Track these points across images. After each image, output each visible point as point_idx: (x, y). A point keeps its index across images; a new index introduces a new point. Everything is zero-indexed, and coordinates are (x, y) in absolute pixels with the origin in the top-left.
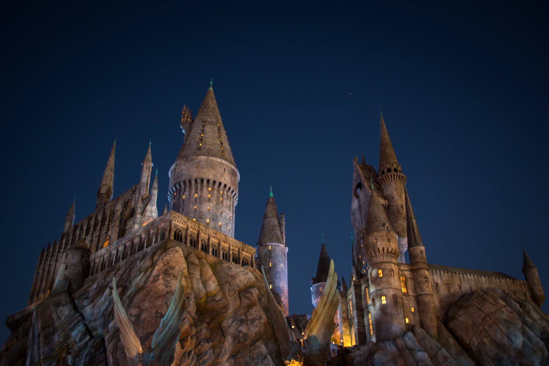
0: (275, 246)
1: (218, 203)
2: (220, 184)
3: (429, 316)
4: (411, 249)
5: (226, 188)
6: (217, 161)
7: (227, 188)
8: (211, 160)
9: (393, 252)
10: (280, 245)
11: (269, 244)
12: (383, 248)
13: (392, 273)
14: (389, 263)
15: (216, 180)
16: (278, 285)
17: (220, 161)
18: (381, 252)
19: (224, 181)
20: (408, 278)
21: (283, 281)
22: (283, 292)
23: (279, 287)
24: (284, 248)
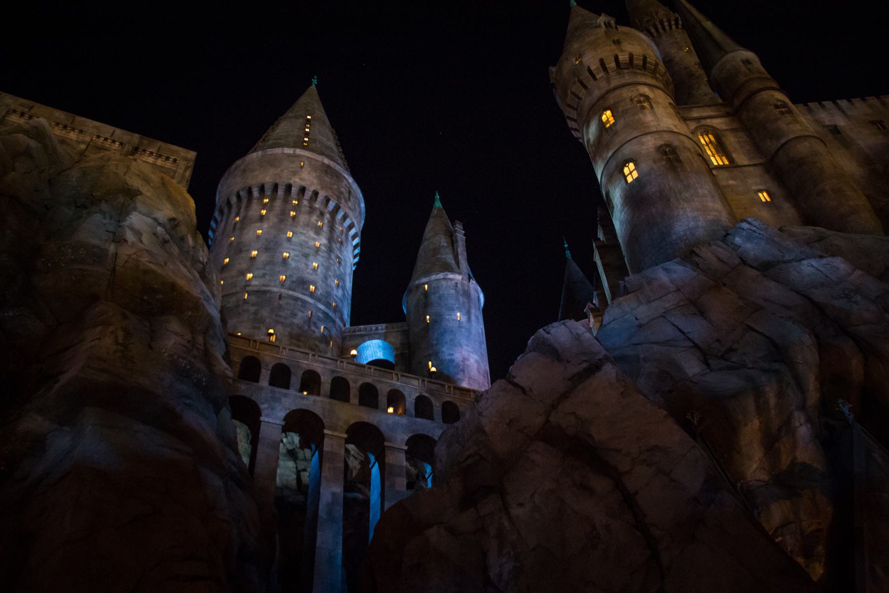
2: (289, 187)
3: (827, 188)
4: (715, 71)
5: (306, 194)
6: (285, 154)
7: (308, 194)
8: (271, 155)
9: (638, 62)
10: (451, 276)
12: (602, 63)
13: (646, 104)
14: (629, 87)
15: (277, 181)
16: (449, 358)
17: (292, 152)
18: (598, 73)
19: (296, 182)
20: (724, 130)
21: (462, 347)
22: (463, 371)
23: (452, 361)
24: (463, 285)
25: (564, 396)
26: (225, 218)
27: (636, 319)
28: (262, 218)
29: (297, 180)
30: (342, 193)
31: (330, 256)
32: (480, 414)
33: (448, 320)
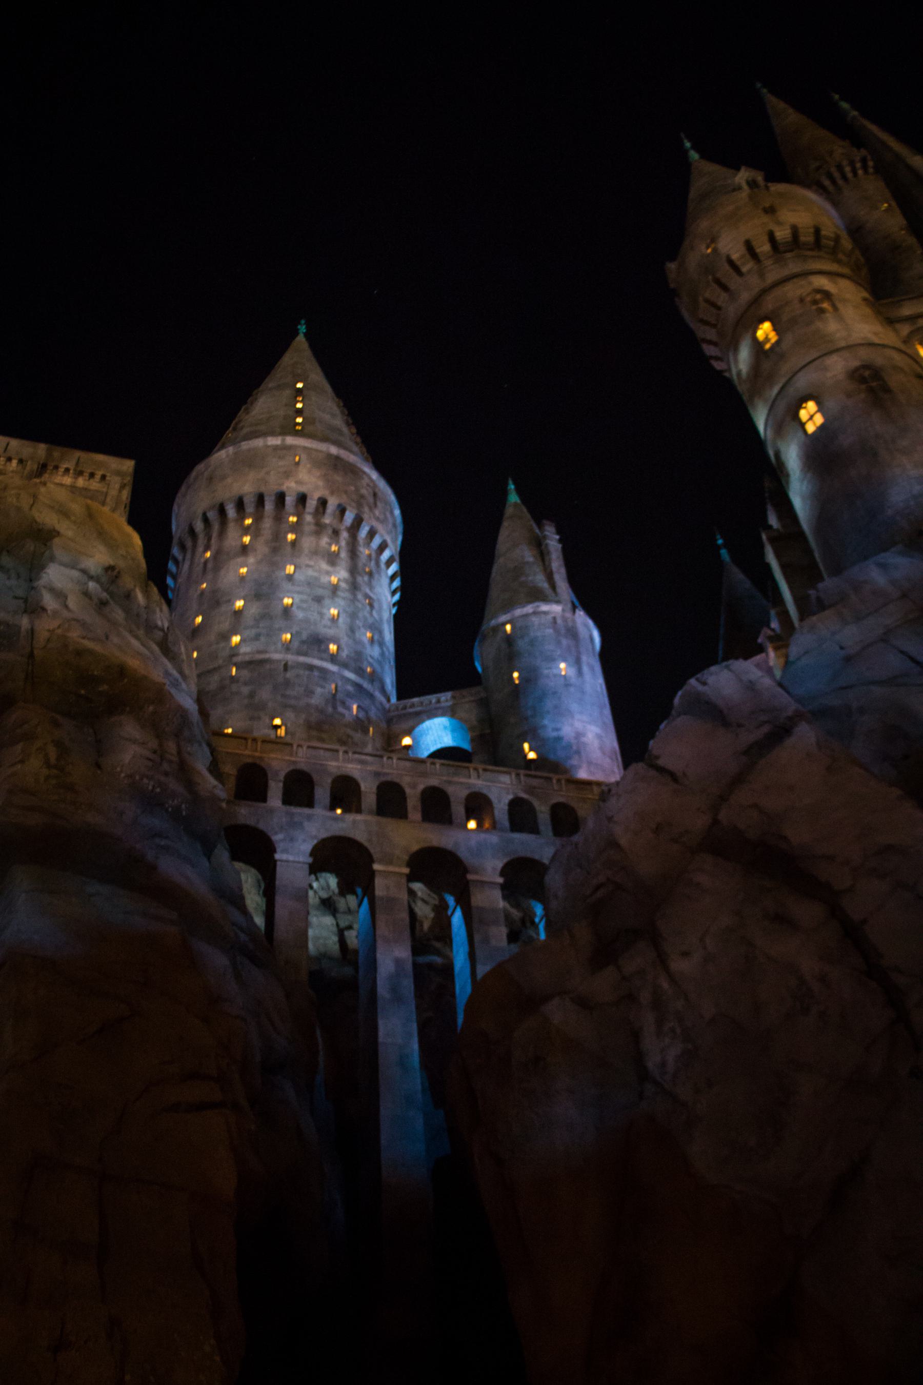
0: (526, 616)
1: (275, 550)
2: (281, 498)
5: (308, 505)
7: (312, 504)
9: (807, 238)
10: (544, 607)
11: (503, 618)
13: (825, 305)
14: (795, 280)
15: (263, 489)
16: (555, 734)
19: (291, 487)
21: (573, 717)
22: (578, 752)
23: (559, 739)
24: (565, 619)
25: (738, 780)
26: (188, 556)
27: (842, 648)
28: (244, 549)
29: (293, 485)
30: (362, 496)
31: (355, 595)
32: (610, 819)
33: (548, 677)
